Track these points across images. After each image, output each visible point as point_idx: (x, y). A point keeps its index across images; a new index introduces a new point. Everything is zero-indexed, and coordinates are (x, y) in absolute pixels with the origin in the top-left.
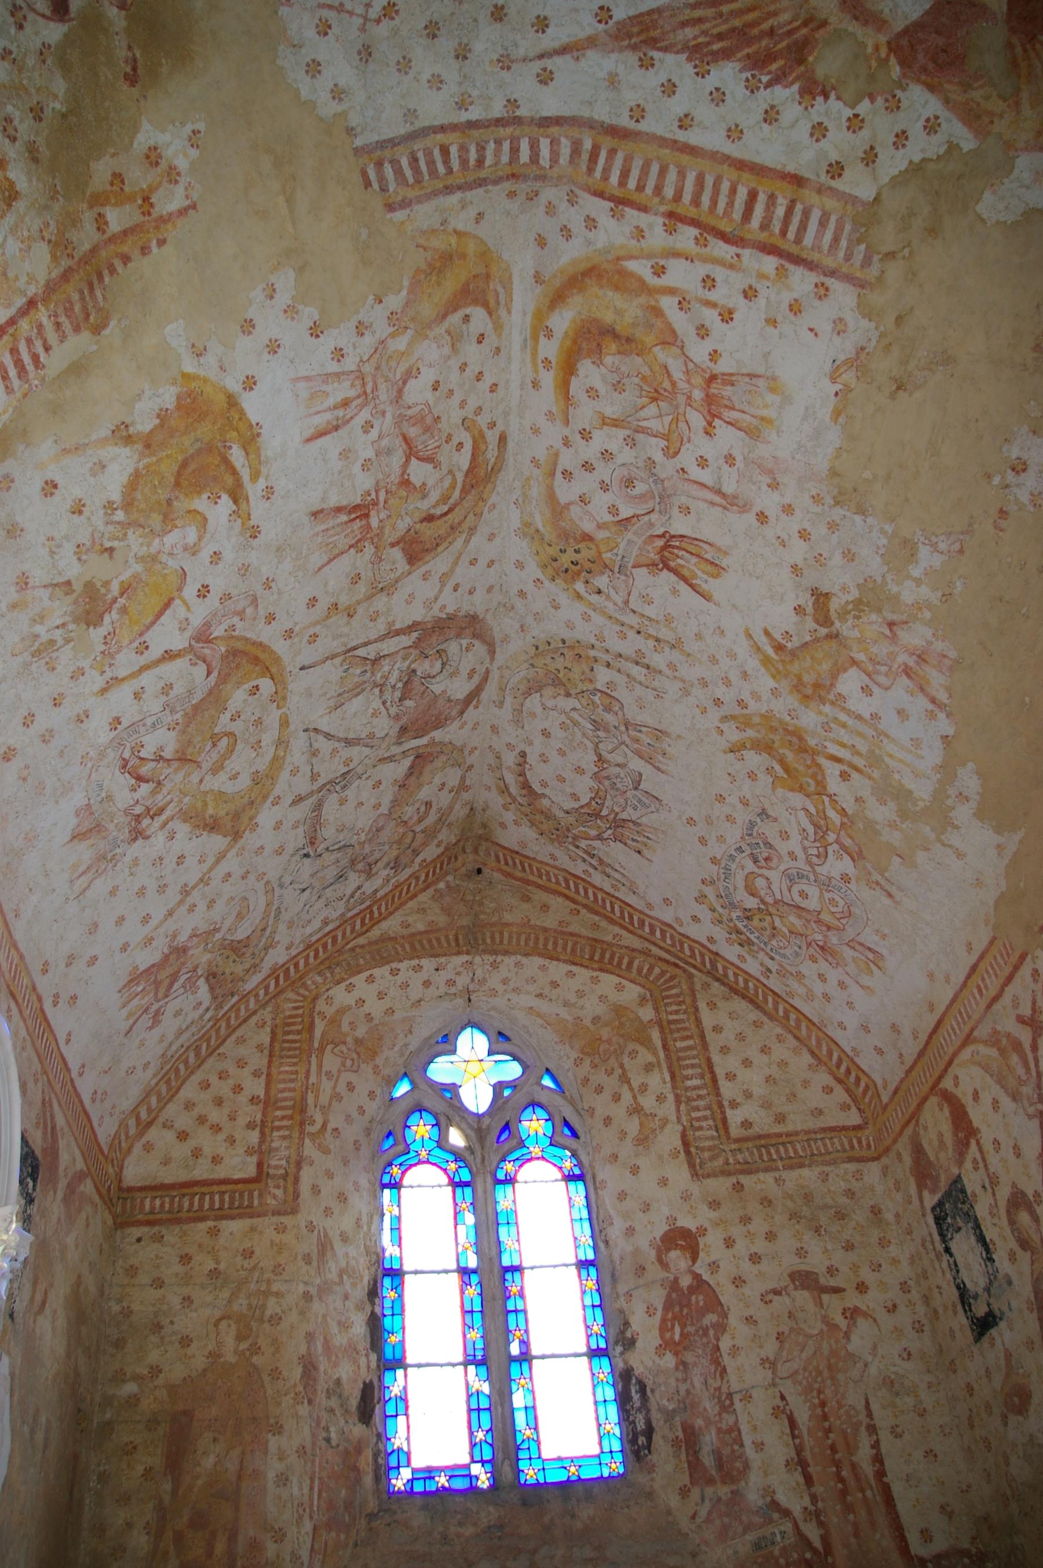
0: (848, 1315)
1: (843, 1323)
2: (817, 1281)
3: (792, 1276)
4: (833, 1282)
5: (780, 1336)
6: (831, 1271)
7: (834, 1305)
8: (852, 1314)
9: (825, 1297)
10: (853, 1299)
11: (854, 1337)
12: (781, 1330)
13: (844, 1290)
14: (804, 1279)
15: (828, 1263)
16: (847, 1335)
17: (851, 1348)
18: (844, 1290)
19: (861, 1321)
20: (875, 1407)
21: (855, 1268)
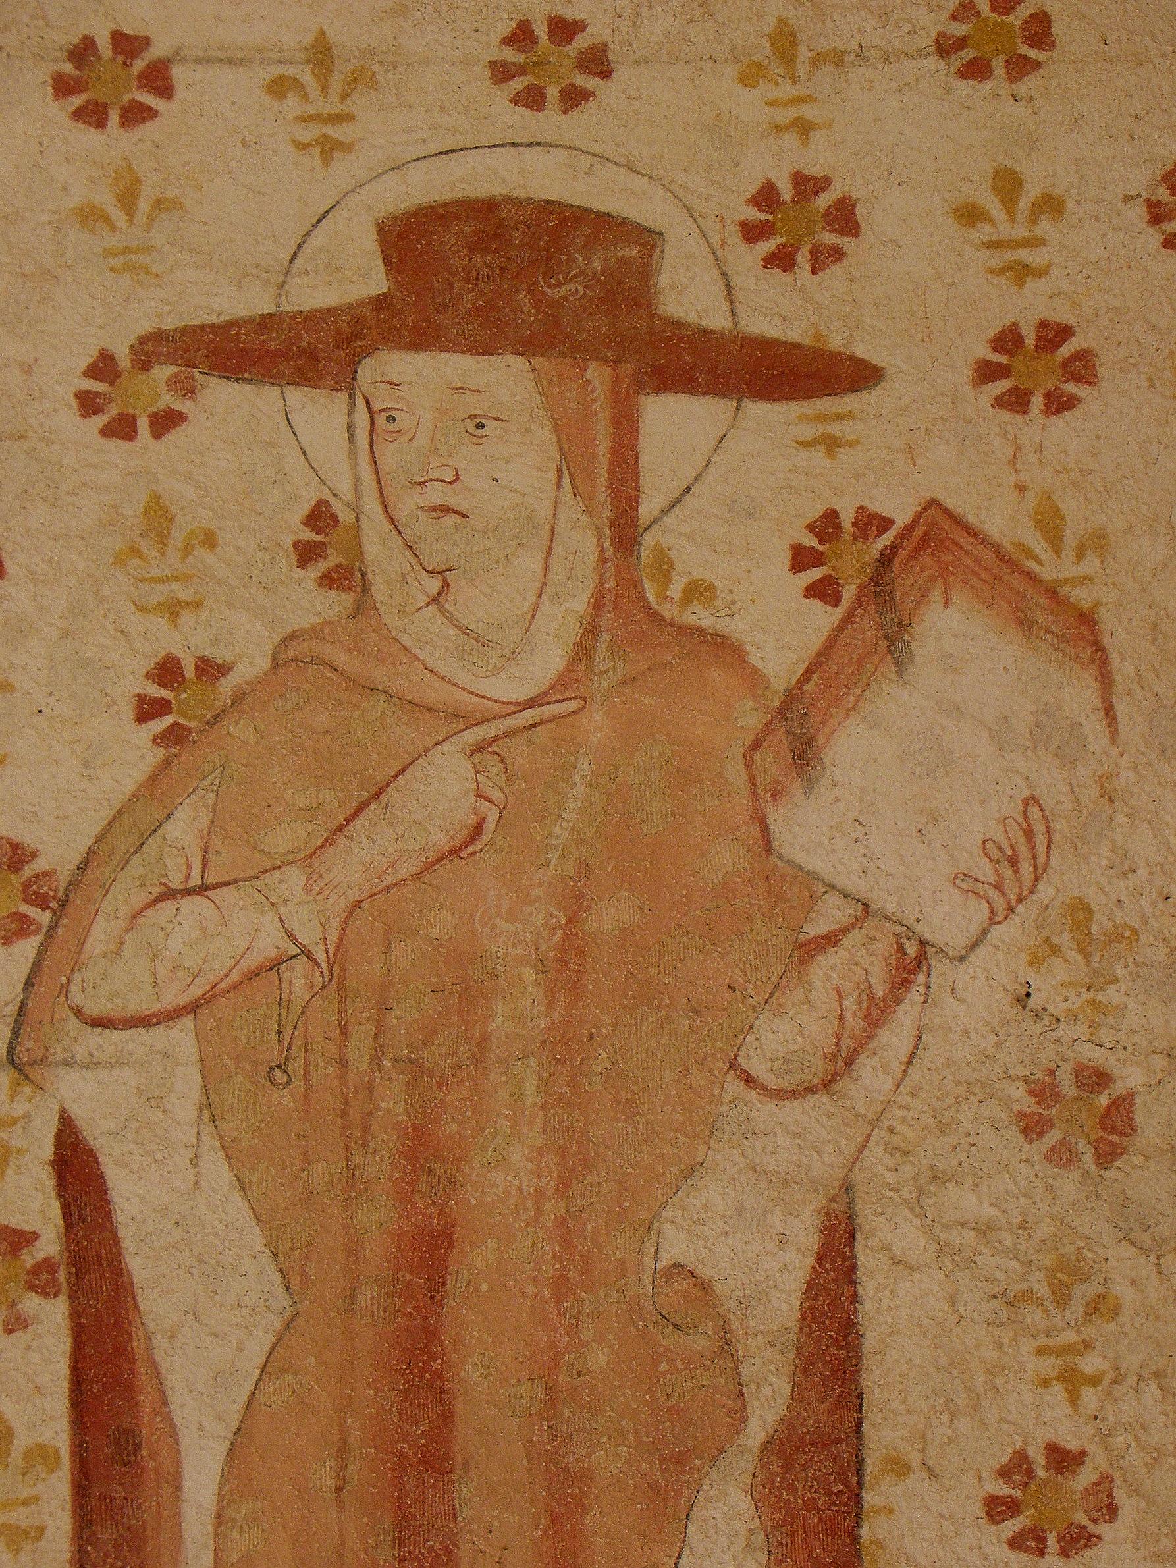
0: (852, 564)
1: (781, 625)
2: (629, 289)
3: (409, 239)
4: (777, 309)
5: (174, 696)
6: (801, 223)
7: (730, 488)
8: (878, 574)
9: (676, 426)
10: (919, 444)
11: (855, 748)
12: (188, 641)
13: (862, 376)
14: (488, 273)
15: (775, 163)
16: (796, 734)
17: (808, 830)
18: (862, 376)
19: (951, 627)
20: (896, 1308)
21: (1008, 208)
